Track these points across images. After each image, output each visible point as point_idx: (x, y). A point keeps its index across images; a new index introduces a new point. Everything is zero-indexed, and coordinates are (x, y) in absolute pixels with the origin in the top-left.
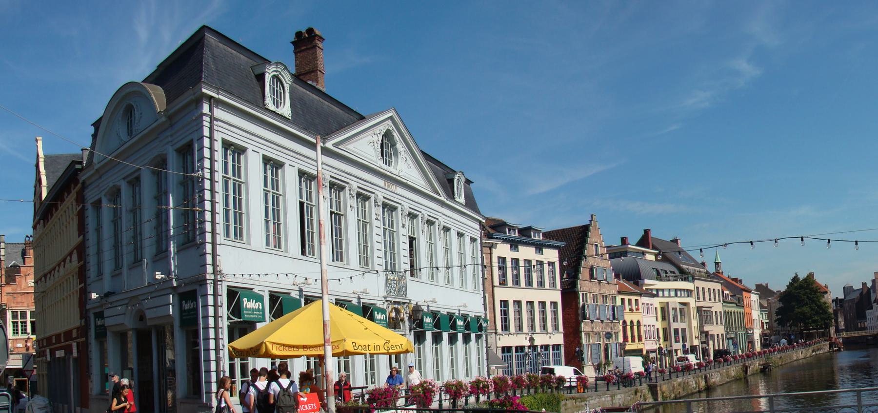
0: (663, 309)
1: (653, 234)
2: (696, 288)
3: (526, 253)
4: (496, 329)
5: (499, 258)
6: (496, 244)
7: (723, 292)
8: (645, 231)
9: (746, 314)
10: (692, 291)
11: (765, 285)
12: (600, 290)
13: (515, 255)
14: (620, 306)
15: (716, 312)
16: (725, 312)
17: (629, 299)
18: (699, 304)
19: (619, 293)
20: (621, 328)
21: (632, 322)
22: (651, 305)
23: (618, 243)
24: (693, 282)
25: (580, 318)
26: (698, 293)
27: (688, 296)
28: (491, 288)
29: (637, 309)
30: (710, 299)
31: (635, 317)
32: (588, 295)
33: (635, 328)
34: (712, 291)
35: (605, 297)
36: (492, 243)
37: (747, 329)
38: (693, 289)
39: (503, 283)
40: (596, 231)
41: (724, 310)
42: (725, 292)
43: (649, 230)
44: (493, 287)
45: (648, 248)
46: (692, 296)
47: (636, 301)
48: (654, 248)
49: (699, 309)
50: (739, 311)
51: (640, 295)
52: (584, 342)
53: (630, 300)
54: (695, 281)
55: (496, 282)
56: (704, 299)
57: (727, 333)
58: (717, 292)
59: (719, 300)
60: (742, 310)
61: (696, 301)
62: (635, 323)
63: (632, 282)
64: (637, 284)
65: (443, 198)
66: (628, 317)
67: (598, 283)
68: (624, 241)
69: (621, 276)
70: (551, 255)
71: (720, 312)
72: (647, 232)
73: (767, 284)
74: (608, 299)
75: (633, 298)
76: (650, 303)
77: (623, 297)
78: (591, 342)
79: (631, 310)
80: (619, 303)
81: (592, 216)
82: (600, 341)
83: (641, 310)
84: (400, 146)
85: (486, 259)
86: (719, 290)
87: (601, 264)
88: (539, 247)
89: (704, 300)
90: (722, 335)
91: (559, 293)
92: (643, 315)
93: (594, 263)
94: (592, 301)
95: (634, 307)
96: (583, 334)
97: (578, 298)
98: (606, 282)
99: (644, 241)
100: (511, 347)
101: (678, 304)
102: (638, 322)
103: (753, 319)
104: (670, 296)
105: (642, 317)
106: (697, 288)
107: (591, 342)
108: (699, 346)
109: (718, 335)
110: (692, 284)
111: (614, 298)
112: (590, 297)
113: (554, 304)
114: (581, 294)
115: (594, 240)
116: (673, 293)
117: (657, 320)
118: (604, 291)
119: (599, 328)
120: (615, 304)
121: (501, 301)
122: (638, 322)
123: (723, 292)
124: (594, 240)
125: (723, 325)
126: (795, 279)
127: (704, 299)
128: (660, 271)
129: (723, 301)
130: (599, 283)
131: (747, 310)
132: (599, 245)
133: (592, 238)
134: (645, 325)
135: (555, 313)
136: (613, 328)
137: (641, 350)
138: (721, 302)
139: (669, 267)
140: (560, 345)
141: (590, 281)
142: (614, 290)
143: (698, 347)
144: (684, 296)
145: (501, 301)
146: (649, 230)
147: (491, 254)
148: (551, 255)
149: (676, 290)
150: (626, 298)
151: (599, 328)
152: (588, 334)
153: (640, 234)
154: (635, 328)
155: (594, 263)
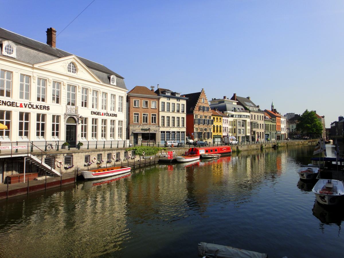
1: (237, 95)
2: (251, 115)
3: (173, 101)
4: (159, 125)
5: (162, 102)
7: (265, 117)
9: (277, 126)
12: (204, 114)
13: (169, 101)
15: (260, 124)
16: (265, 124)
17: (217, 118)
18: (252, 121)
19: (212, 115)
20: (212, 127)
21: (217, 126)
22: (227, 120)
23: (222, 98)
24: (250, 112)
25: (194, 123)
26: (252, 117)
27: (246, 118)
31: (219, 124)
32: (198, 115)
33: (219, 128)
34: (259, 116)
35: (206, 117)
37: (277, 131)
38: (249, 115)
39: (163, 110)
40: (204, 94)
42: (266, 117)
44: (159, 111)
45: (235, 100)
46: (249, 118)
47: (220, 119)
48: (237, 100)
52: (195, 131)
53: (217, 119)
55: (160, 110)
56: (255, 119)
57: (265, 132)
58: (261, 116)
59: (263, 120)
60: (275, 124)
62: (219, 126)
63: (221, 112)
64: (223, 112)
65: (101, 83)
68: (225, 97)
69: (216, 110)
71: (263, 124)
72: (235, 94)
75: (219, 118)
80: (212, 118)
81: (202, 89)
84: (79, 67)
86: (263, 116)
88: (178, 99)
90: (263, 133)
91: (185, 115)
96: (195, 129)
99: (234, 98)
102: (220, 126)
103: (281, 127)
107: (198, 131)
108: (250, 136)
110: (249, 114)
111: (210, 117)
114: (195, 115)
116: (240, 116)
118: (205, 115)
122: (220, 126)
123: (265, 117)
127: (255, 119)
129: (265, 120)
130: (203, 112)
131: (278, 124)
133: (201, 96)
134: (224, 127)
137: (221, 136)
139: (241, 107)
140: (184, 132)
141: (199, 111)
142: (210, 114)
144: (245, 118)
145: (162, 116)
147: (159, 101)
148: (184, 102)
150: (216, 117)
152: (197, 129)
153: (232, 96)
154: (219, 128)
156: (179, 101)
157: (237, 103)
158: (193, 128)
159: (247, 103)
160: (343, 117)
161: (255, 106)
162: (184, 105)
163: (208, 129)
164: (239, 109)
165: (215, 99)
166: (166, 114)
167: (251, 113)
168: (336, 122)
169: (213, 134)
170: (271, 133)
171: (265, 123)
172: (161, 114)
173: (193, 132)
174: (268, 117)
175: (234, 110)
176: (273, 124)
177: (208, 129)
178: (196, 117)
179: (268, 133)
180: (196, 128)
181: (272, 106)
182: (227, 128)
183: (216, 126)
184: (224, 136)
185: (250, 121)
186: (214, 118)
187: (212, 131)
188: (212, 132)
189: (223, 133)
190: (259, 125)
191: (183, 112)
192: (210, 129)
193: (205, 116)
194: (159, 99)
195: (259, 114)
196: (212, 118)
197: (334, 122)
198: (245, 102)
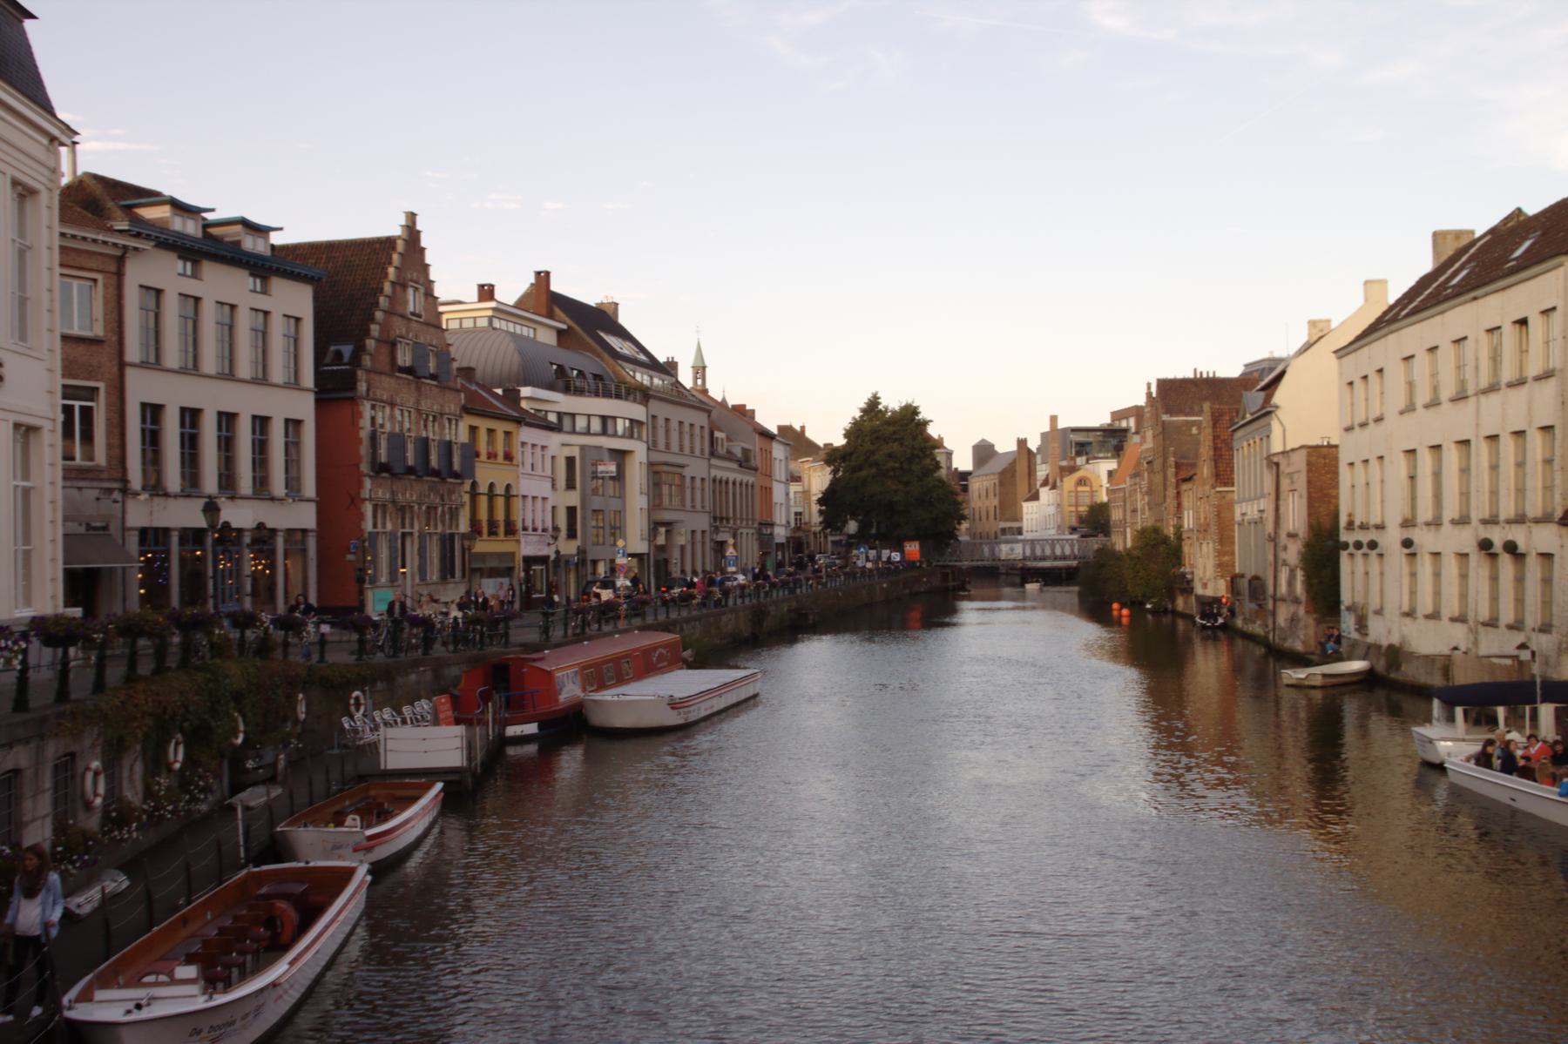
0: (570, 461)
4: (124, 480)
6: (136, 249)
8: (538, 273)
10: (640, 423)
11: (798, 429)
12: (418, 402)
15: (693, 478)
16: (714, 480)
18: (657, 457)
19: (467, 410)
20: (466, 498)
21: (492, 486)
22: (543, 448)
26: (654, 428)
27: (631, 436)
28: (115, 369)
30: (681, 448)
34: (686, 428)
36: (125, 247)
38: (643, 418)
41: (713, 475)
42: (717, 434)
43: (548, 274)
44: (122, 365)
46: (640, 438)
49: (657, 468)
50: (745, 481)
51: (519, 421)
52: (368, 526)
53: (491, 431)
54: (652, 403)
55: (133, 352)
56: (668, 446)
59: (702, 451)
61: (648, 449)
62: (500, 490)
67: (413, 386)
70: (294, 300)
71: (703, 479)
72: (543, 278)
73: (803, 428)
74: (436, 424)
75: (501, 427)
76: (541, 442)
77: (476, 421)
78: (389, 527)
80: (463, 437)
82: (412, 526)
83: (518, 457)
85: (106, 286)
90: (703, 532)
93: (408, 332)
96: (368, 509)
97: (360, 415)
100: (166, 531)
102: (508, 487)
104: (588, 432)
105: (518, 477)
109: (693, 532)
113: (293, 425)
115: (409, 276)
116: (596, 425)
117: (553, 486)
119: (411, 495)
121: (144, 406)
122: (508, 487)
124: (409, 276)
125: (707, 509)
128: (569, 371)
129: (713, 454)
134: (524, 497)
135: (293, 446)
136: (446, 497)
140: (304, 531)
143: (646, 557)
145: (144, 406)
146: (548, 274)
147: (120, 274)
148: (294, 300)
149: (604, 419)
150: (483, 424)
151: (411, 495)
155: (408, 332)
156: (265, 291)
157: (560, 332)
158: (355, 501)
160: (993, 446)
161: (653, 365)
162: (298, 320)
164: (581, 373)
166: (174, 394)
167: (655, 406)
171: (714, 472)
172: (141, 388)
175: (561, 383)
177: (443, 512)
180: (375, 507)
183: (483, 488)
184: (529, 561)
185: (645, 460)
189: (522, 540)
192: (454, 514)
194: (121, 261)
198: (602, 334)
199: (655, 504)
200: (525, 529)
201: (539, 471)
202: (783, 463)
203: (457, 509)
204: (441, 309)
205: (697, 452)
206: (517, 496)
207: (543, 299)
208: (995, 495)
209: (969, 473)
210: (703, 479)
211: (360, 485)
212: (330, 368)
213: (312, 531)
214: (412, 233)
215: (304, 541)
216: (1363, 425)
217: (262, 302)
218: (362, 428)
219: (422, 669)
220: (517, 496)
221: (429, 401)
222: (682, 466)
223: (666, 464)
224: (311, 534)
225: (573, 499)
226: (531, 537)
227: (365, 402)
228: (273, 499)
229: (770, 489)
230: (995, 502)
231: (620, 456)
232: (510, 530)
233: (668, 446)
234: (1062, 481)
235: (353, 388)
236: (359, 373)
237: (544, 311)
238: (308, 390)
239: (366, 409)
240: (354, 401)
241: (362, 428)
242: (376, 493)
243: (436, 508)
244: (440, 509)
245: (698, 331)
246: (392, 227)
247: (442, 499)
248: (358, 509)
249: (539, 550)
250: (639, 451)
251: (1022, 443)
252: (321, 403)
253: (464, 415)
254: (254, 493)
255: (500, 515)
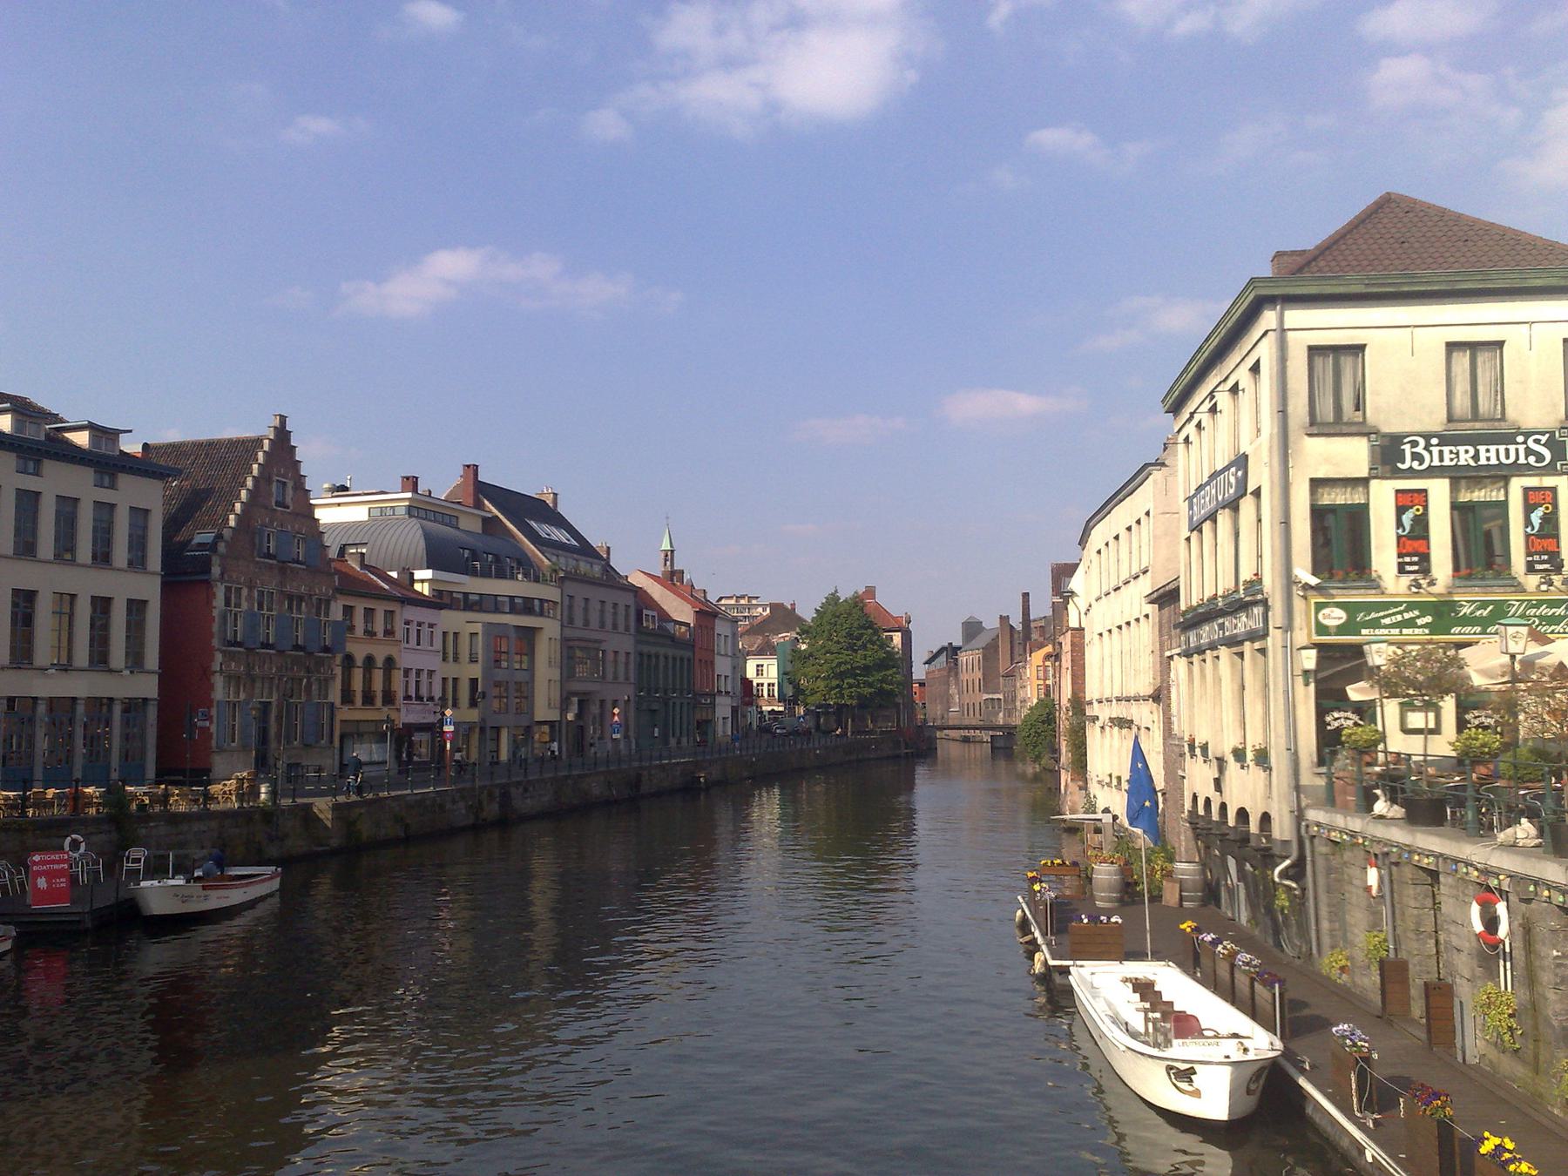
2: (566, 600)
10: (555, 603)
11: (789, 607)
14: (336, 622)
16: (641, 654)
18: (569, 633)
20: (338, 671)
21: (370, 660)
22: (431, 626)
26: (571, 607)
27: (541, 614)
29: (389, 632)
32: (245, 592)
33: (378, 676)
34: (609, 608)
35: (295, 600)
38: (559, 601)
47: (389, 614)
49: (571, 644)
53: (369, 613)
56: (587, 623)
59: (627, 628)
60: (687, 654)
61: (562, 626)
62: (380, 662)
66: (359, 652)
71: (628, 654)
72: (473, 469)
73: (793, 605)
74: (304, 604)
75: (380, 608)
76: (427, 621)
79: (370, 633)
80: (336, 612)
83: (399, 634)
86: (627, 607)
87: (293, 527)
89: (626, 631)
91: (158, 581)
92: (407, 646)
93: (271, 522)
94: (256, 605)
95: (379, 627)
96: (219, 682)
98: (304, 567)
101: (513, 630)
102: (390, 662)
106: (571, 597)
111: (324, 604)
112: (250, 598)
113: (136, 607)
117: (444, 659)
120: (327, 615)
125: (632, 680)
126: (833, 599)
132: (290, 484)
134: (407, 672)
138: (632, 630)
140: (145, 700)
143: (557, 724)
150: (360, 606)
151: (271, 669)
154: (378, 676)
158: (206, 673)
159: (545, 530)
162: (146, 512)
163: (309, 684)
165: (344, 488)
168: (952, 651)
169: (344, 713)
170: (666, 704)
173: (209, 703)
174: (655, 614)
176: (679, 653)
178: (228, 603)
179: (655, 706)
181: (669, 556)
182: (431, 673)
184: (410, 729)
185: (559, 637)
186: (348, 611)
187: (335, 695)
188: (338, 702)
189: (403, 710)
190: (610, 657)
191: (137, 562)
192: (325, 684)
193: (290, 598)
195: (610, 596)
196: (336, 612)
197: (943, 649)
199: (568, 673)
200: (408, 697)
201: (425, 645)
202: (730, 640)
203: (326, 680)
204: (312, 502)
205: (621, 628)
206: (400, 669)
207: (471, 489)
208: (979, 669)
209: (960, 648)
210: (628, 654)
211: (212, 659)
212: (192, 553)
213: (155, 699)
214: (282, 435)
215: (110, 710)
216: (1088, 610)
217: (106, 496)
218: (215, 608)
219: (152, 824)
220: (400, 669)
221: (295, 584)
222: (600, 642)
223: (580, 640)
224: (152, 702)
225: (476, 671)
226: (413, 706)
227: (219, 584)
228: (111, 671)
229: (712, 663)
230: (979, 675)
231: (529, 634)
232: (389, 698)
233: (587, 623)
234: (1030, 656)
235: (208, 571)
236: (216, 560)
237: (470, 501)
238: (154, 573)
239: (220, 591)
240: (208, 584)
241: (215, 608)
242: (229, 666)
243: (301, 680)
244: (305, 680)
245: (667, 518)
246: (264, 429)
247: (308, 670)
248: (209, 680)
249: (424, 718)
250: (550, 628)
251: (1004, 619)
252: (167, 587)
253: (338, 596)
254: (90, 666)
255: (378, 685)
